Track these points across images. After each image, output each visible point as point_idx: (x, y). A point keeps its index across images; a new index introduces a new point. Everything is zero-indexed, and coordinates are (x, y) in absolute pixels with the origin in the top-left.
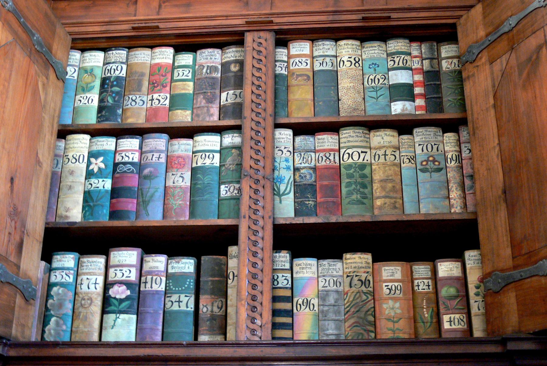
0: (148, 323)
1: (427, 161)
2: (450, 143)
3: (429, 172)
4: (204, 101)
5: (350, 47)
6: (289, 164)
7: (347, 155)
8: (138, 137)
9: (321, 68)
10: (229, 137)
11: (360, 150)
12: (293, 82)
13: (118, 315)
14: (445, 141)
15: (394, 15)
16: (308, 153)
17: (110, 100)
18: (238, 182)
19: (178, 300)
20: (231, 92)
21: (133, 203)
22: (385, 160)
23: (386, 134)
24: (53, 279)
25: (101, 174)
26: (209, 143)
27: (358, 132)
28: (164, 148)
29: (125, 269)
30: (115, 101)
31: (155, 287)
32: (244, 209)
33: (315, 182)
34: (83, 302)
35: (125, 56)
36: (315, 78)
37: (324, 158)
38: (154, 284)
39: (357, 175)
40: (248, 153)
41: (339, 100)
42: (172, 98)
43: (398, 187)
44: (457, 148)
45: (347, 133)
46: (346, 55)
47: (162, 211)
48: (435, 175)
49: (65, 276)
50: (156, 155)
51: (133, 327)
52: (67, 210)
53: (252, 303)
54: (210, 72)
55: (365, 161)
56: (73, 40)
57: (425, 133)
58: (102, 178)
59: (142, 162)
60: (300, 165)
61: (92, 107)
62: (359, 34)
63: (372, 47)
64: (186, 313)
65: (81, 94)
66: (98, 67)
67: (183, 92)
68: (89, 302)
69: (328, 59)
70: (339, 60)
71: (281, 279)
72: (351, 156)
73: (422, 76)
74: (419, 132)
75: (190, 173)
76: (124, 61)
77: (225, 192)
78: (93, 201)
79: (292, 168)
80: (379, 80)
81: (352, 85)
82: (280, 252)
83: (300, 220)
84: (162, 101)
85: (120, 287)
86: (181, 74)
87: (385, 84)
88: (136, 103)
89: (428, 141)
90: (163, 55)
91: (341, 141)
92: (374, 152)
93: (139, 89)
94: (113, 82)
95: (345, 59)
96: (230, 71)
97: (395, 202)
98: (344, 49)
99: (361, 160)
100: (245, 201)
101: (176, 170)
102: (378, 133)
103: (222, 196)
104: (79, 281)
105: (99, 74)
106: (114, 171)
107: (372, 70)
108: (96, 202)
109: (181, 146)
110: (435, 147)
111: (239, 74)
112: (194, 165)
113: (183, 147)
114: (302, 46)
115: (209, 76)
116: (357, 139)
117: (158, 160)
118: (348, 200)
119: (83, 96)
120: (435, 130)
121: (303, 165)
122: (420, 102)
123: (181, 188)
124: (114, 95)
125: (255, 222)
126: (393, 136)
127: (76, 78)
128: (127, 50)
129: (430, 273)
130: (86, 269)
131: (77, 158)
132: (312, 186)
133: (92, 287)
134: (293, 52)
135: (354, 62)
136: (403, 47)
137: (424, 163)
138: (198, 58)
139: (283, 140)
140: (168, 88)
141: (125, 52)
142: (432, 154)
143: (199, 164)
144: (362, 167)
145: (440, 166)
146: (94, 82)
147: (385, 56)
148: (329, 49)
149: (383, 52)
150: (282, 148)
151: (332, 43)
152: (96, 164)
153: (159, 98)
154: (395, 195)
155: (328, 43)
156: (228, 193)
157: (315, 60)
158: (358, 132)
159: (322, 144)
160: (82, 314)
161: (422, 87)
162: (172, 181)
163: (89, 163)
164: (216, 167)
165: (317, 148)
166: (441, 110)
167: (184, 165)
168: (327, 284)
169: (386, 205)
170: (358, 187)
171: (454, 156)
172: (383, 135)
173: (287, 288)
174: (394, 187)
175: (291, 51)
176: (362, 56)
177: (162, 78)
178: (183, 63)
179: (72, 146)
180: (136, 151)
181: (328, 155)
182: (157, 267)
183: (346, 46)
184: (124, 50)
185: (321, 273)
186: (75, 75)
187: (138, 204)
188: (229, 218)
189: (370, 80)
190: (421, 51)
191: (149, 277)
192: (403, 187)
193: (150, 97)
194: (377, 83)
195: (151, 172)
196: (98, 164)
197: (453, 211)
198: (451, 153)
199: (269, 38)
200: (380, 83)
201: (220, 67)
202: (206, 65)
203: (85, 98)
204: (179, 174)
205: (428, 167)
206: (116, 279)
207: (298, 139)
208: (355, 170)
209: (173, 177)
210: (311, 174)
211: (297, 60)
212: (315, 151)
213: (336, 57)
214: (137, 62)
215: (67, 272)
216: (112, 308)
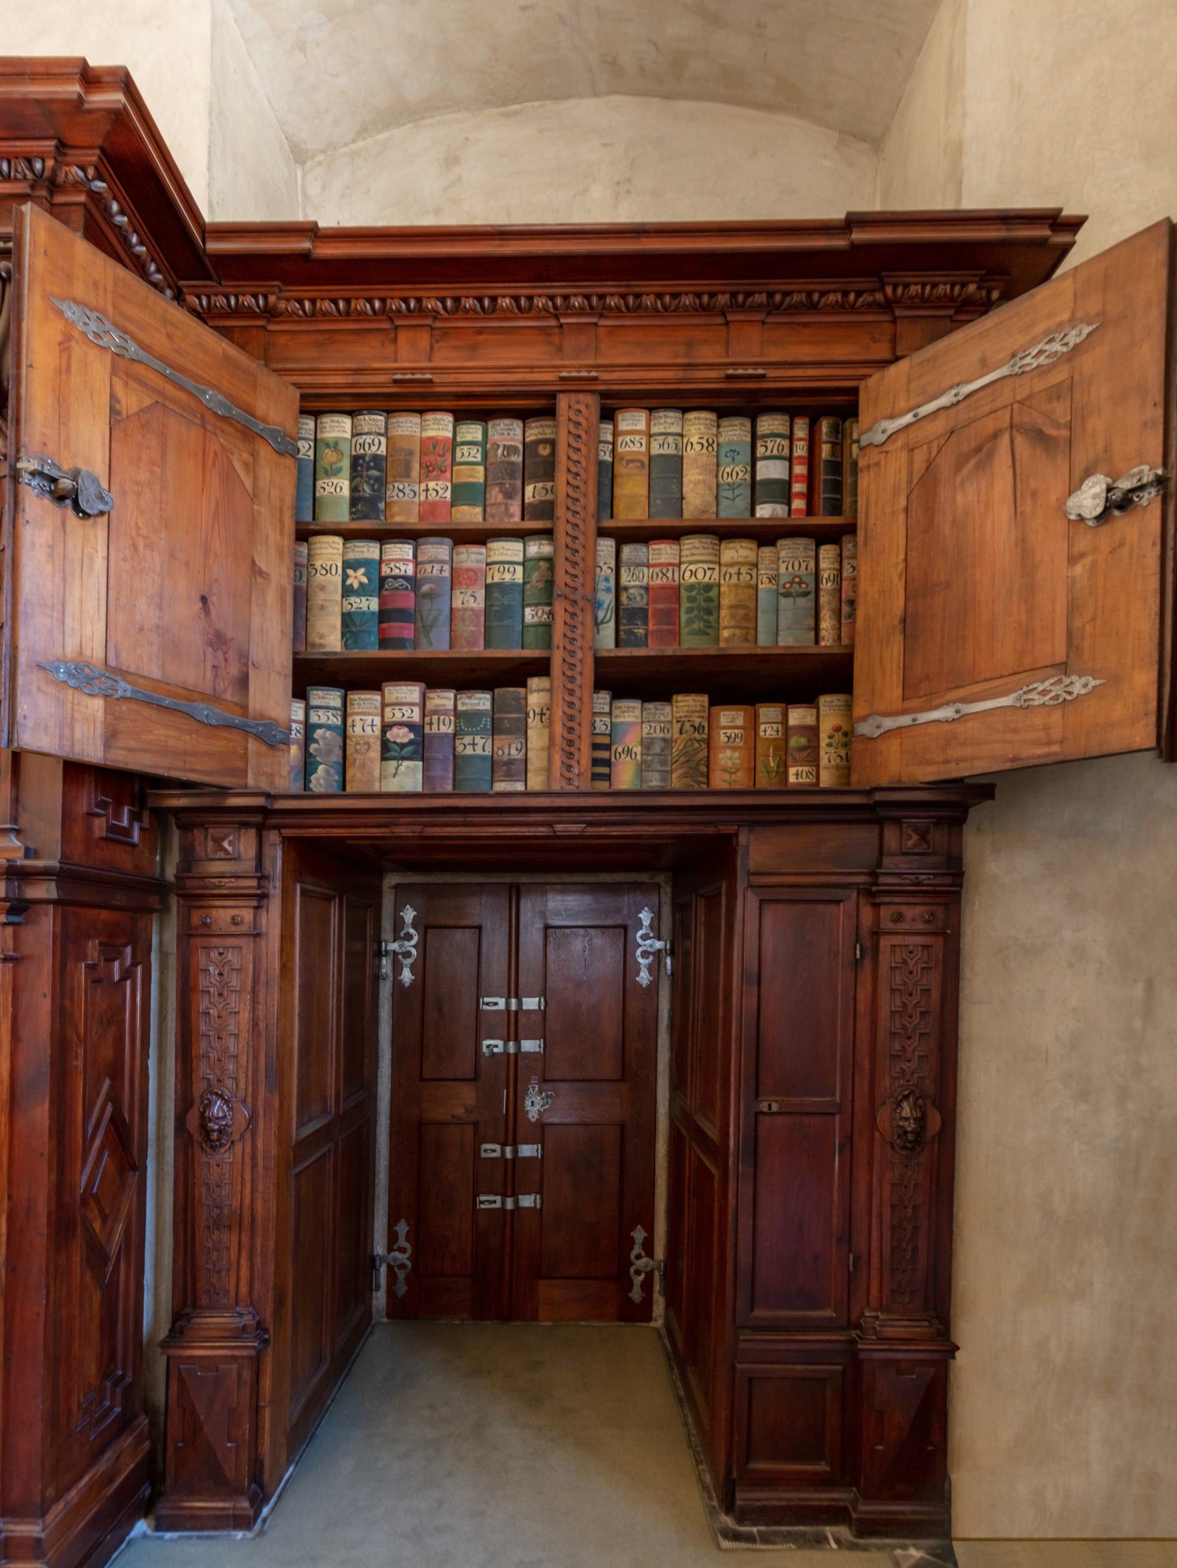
0: (437, 771)
4: (500, 496)
5: (702, 422)
8: (410, 541)
9: (662, 451)
12: (620, 469)
15: (771, 373)
17: (367, 488)
18: (550, 604)
21: (410, 629)
26: (509, 552)
28: (447, 558)
30: (374, 490)
32: (558, 638)
33: (647, 604)
36: (652, 465)
40: (561, 566)
41: (682, 498)
42: (456, 488)
43: (752, 615)
44: (837, 566)
47: (448, 639)
50: (437, 567)
53: (567, 748)
54: (509, 455)
56: (303, 397)
58: (364, 596)
59: (418, 576)
61: (342, 497)
62: (717, 403)
64: (483, 758)
66: (345, 439)
67: (470, 480)
69: (670, 439)
71: (598, 724)
72: (694, 573)
75: (483, 592)
76: (383, 431)
78: (355, 625)
81: (701, 477)
84: (441, 492)
86: (466, 454)
89: (795, 557)
90: (438, 424)
91: (684, 553)
92: (724, 569)
93: (407, 474)
94: (368, 463)
95: (694, 440)
97: (747, 633)
98: (694, 425)
100: (559, 629)
102: (731, 545)
103: (526, 621)
105: (345, 448)
108: (360, 626)
110: (804, 565)
111: (550, 459)
112: (489, 581)
113: (473, 557)
115: (506, 459)
116: (702, 551)
119: (327, 481)
123: (472, 610)
124: (372, 482)
125: (572, 653)
128: (385, 414)
129: (780, 717)
131: (328, 568)
134: (623, 426)
137: (788, 585)
140: (448, 474)
141: (382, 418)
143: (496, 580)
144: (708, 587)
145: (808, 590)
146: (340, 461)
148: (673, 424)
151: (677, 415)
152: (356, 577)
153: (436, 487)
154: (747, 625)
157: (652, 439)
161: (803, 482)
162: (460, 601)
164: (517, 584)
167: (476, 580)
170: (702, 613)
177: (439, 458)
178: (469, 438)
180: (409, 560)
182: (445, 705)
183: (696, 421)
187: (416, 630)
188: (537, 648)
192: (759, 614)
193: (423, 486)
195: (431, 589)
196: (358, 577)
198: (828, 572)
199: (588, 405)
202: (501, 444)
203: (330, 484)
204: (470, 592)
209: (462, 596)
210: (642, 596)
211: (628, 438)
212: (648, 566)
213: (682, 435)
214: (400, 433)
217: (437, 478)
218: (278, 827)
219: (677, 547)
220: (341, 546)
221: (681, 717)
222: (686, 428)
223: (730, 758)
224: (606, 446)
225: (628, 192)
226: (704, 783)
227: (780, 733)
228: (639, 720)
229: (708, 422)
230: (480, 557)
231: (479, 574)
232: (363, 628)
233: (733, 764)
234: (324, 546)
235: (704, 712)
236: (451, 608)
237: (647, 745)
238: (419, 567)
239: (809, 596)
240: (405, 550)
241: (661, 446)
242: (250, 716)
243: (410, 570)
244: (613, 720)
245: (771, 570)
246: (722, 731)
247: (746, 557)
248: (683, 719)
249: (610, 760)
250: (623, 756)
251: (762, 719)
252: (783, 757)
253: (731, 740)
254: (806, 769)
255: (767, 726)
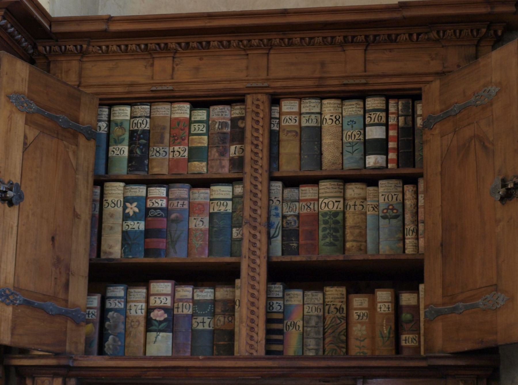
9: (308, 124)
11: (334, 200)
25: (135, 217)
28: (187, 196)
29: (162, 297)
30: (142, 152)
34: (133, 324)
37: (306, 207)
38: (184, 310)
39: (331, 221)
42: (191, 150)
49: (117, 303)
50: (181, 202)
52: (111, 247)
55: (338, 209)
69: (313, 116)
83: (287, 258)
84: (182, 152)
86: (197, 129)
91: (321, 191)
94: (140, 135)
99: (335, 209)
104: (128, 307)
118: (323, 242)
123: (201, 230)
133: (139, 312)
135: (334, 120)
140: (186, 141)
142: (392, 203)
155: (313, 101)
157: (302, 116)
162: (194, 224)
163: (125, 208)
178: (198, 118)
179: (110, 192)
181: (309, 204)
187: (167, 243)
195: (177, 217)
205: (388, 214)
206: (156, 305)
211: (288, 117)
216: (154, 328)
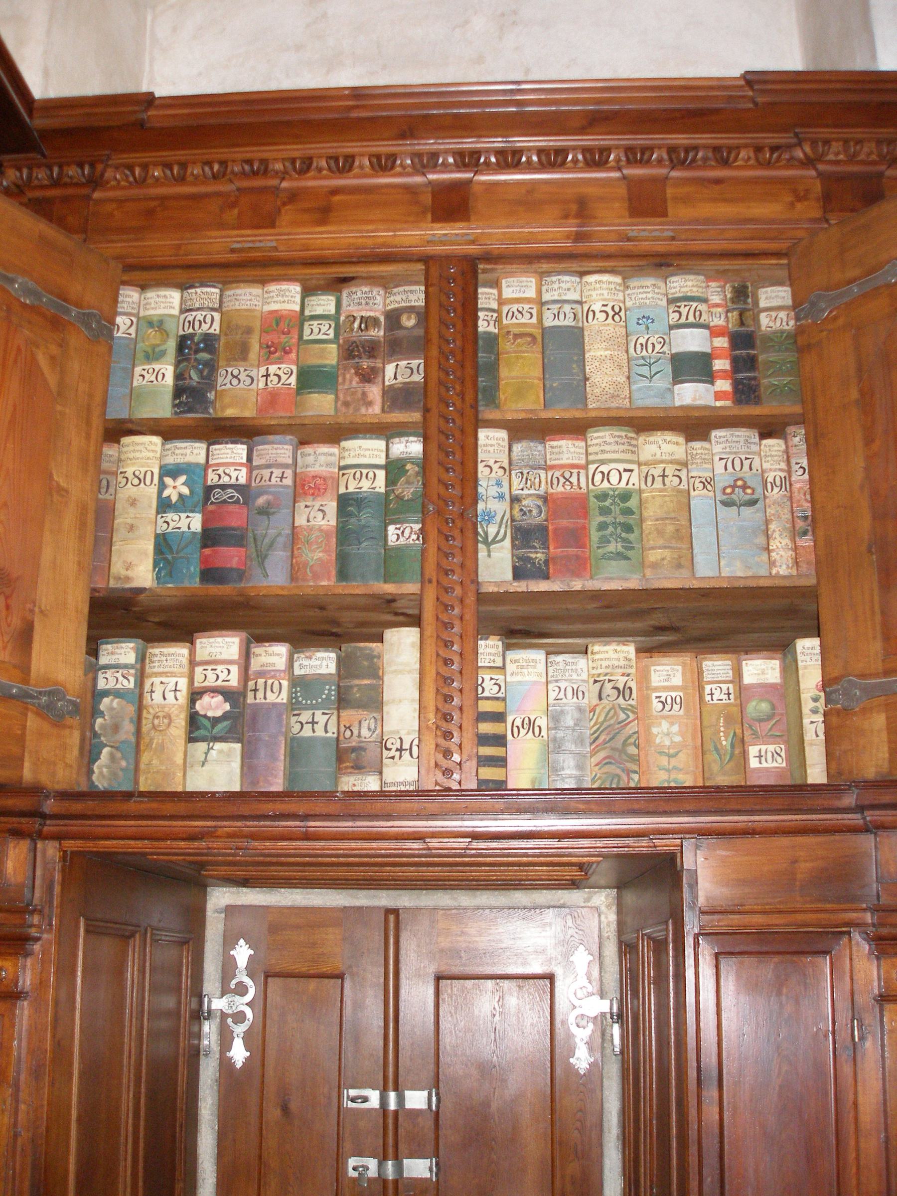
1: (734, 487)
2: (772, 456)
3: (736, 505)
4: (356, 379)
5: (604, 286)
6: (502, 490)
7: (600, 475)
9: (556, 323)
10: (400, 442)
11: (621, 467)
12: (506, 346)
13: (211, 744)
14: (763, 454)
16: (535, 471)
19: (310, 720)
20: (403, 363)
22: (664, 484)
23: (665, 440)
24: (101, 685)
25: (183, 505)
26: (367, 453)
27: (619, 436)
28: (290, 461)
30: (202, 377)
31: (271, 698)
33: (546, 520)
35: (218, 297)
37: (562, 480)
39: (616, 510)
45: (599, 437)
46: (598, 300)
48: (747, 511)
50: (277, 472)
51: (236, 765)
52: (129, 566)
55: (630, 486)
57: (730, 440)
58: (185, 512)
60: (521, 492)
63: (642, 287)
65: (143, 364)
68: (166, 721)
69: (567, 308)
70: (585, 309)
72: (606, 476)
73: (726, 339)
74: (720, 437)
75: (334, 504)
76: (217, 306)
77: (396, 536)
79: (507, 497)
80: (653, 345)
82: (487, 639)
83: (521, 586)
84: (284, 377)
85: (213, 697)
86: (316, 330)
87: (664, 353)
88: (239, 381)
89: (735, 453)
90: (283, 296)
91: (590, 450)
94: (198, 344)
95: (597, 307)
96: (400, 327)
98: (595, 289)
101: (311, 498)
102: (651, 439)
103: (390, 543)
106: (207, 498)
107: (643, 327)
108: (177, 553)
109: (320, 457)
110: (747, 463)
112: (342, 490)
113: (322, 459)
114: (523, 284)
116: (616, 448)
117: (281, 481)
119: (146, 367)
120: (747, 434)
121: (526, 492)
122: (724, 385)
123: (320, 530)
126: (677, 443)
127: (133, 336)
128: (220, 286)
130: (159, 667)
131: (142, 477)
132: (542, 529)
134: (507, 293)
135: (611, 313)
136: (695, 289)
137: (729, 490)
138: (345, 302)
139: (491, 449)
141: (217, 291)
143: (351, 489)
144: (625, 496)
145: (755, 497)
147: (664, 303)
148: (569, 289)
149: (660, 297)
150: (491, 463)
151: (573, 279)
152: (175, 487)
155: (566, 278)
156: (402, 539)
158: (619, 436)
159: (557, 456)
160: (155, 741)
161: (726, 358)
162: (305, 517)
163: (162, 486)
165: (548, 463)
166: (758, 401)
167: (325, 489)
168: (562, 695)
169: (665, 562)
170: (619, 530)
171: (778, 479)
172: (660, 442)
173: (497, 699)
174: (677, 530)
175: (504, 293)
176: (624, 302)
178: (319, 311)
180: (241, 464)
181: (567, 475)
183: (598, 285)
184: (214, 287)
185: (552, 676)
186: (132, 331)
189: (638, 346)
190: (726, 296)
191: (261, 681)
193: (263, 370)
194: (650, 350)
195: (269, 503)
197: (774, 572)
200: (656, 351)
201: (382, 319)
203: (151, 371)
204: (317, 505)
207: (517, 448)
208: (614, 501)
209: (307, 510)
210: (539, 507)
211: (515, 307)
212: (547, 468)
214: (238, 308)
215: (125, 672)
217: (280, 361)
218: (58, 837)
219: (583, 444)
220: (159, 448)
221: (599, 675)
222: (585, 293)
223: (668, 734)
224: (490, 314)
225: (514, 23)
226: (636, 772)
227: (732, 697)
228: (544, 680)
229: (613, 286)
230: (332, 459)
231: (329, 482)
232: (181, 554)
233: (672, 742)
234: (131, 448)
235: (631, 667)
236: (294, 527)
237: (555, 719)
238: (255, 473)
239: (757, 506)
240: (239, 451)
241: (556, 316)
242: (32, 682)
243: (242, 476)
244: (509, 679)
245: (706, 470)
246: (654, 695)
247: (672, 454)
248: (601, 678)
249: (504, 737)
250: (523, 732)
251: (707, 677)
252: (739, 731)
253: (668, 707)
254: (771, 748)
255: (714, 686)
